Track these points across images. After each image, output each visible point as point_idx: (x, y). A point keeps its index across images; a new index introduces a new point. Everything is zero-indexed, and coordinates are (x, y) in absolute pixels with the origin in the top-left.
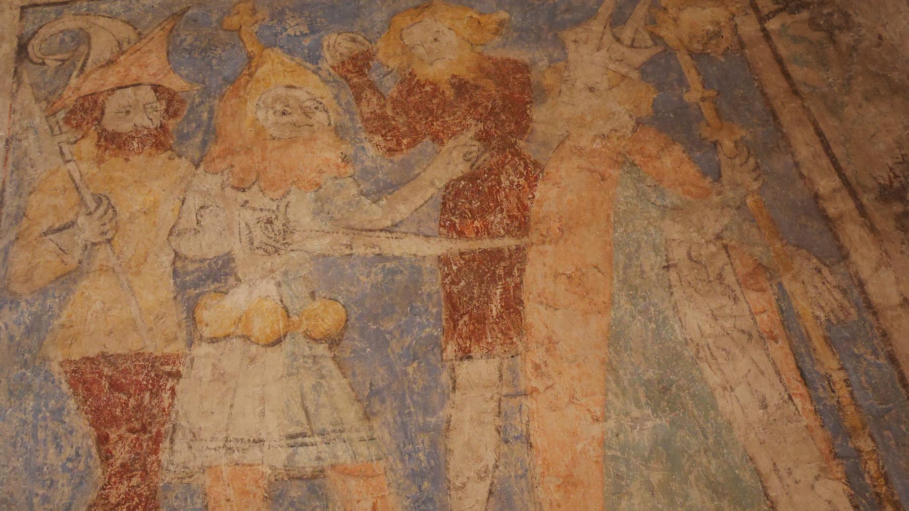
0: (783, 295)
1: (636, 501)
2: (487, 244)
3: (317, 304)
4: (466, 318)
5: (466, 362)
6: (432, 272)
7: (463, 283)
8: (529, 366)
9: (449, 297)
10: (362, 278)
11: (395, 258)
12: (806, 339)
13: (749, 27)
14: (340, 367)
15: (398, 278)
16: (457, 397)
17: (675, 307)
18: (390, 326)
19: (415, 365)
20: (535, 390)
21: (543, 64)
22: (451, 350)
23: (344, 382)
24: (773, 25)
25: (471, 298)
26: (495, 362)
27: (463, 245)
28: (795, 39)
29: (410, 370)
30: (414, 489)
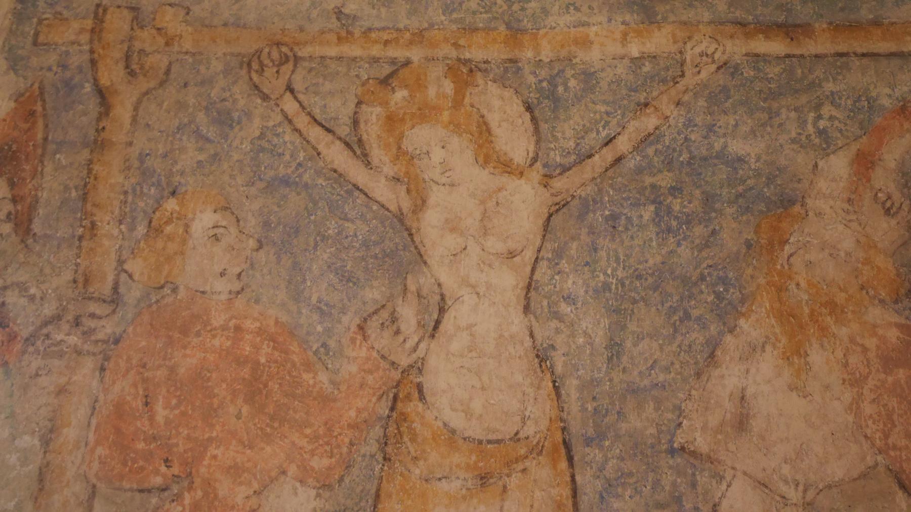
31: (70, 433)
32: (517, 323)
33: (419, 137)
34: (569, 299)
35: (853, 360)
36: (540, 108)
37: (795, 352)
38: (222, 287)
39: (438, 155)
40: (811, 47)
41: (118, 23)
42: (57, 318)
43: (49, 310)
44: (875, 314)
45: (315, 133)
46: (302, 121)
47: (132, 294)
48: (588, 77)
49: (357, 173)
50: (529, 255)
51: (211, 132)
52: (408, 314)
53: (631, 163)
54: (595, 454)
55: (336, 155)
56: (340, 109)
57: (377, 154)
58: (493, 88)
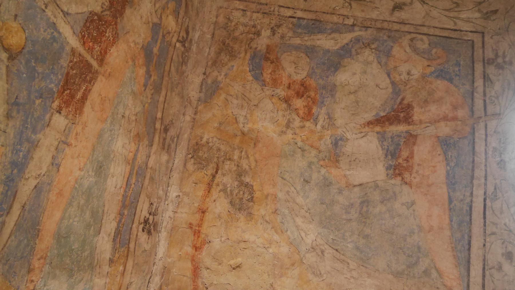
0: (137, 150)
1: (73, 210)
2: (88, 58)
3: (15, 25)
4: (68, 91)
5: (58, 114)
6: (67, 54)
7: (74, 72)
8: (75, 132)
9: (68, 73)
10: (42, 30)
11: (59, 33)
12: (134, 169)
14: (8, 76)
15: (55, 44)
16: (47, 130)
17: (118, 135)
18: (40, 70)
19: (40, 101)
20: (71, 145)
22: (56, 103)
23: (6, 86)
25: (74, 83)
26: (66, 121)
27: (81, 50)
29: (38, 102)
30: (10, 171)
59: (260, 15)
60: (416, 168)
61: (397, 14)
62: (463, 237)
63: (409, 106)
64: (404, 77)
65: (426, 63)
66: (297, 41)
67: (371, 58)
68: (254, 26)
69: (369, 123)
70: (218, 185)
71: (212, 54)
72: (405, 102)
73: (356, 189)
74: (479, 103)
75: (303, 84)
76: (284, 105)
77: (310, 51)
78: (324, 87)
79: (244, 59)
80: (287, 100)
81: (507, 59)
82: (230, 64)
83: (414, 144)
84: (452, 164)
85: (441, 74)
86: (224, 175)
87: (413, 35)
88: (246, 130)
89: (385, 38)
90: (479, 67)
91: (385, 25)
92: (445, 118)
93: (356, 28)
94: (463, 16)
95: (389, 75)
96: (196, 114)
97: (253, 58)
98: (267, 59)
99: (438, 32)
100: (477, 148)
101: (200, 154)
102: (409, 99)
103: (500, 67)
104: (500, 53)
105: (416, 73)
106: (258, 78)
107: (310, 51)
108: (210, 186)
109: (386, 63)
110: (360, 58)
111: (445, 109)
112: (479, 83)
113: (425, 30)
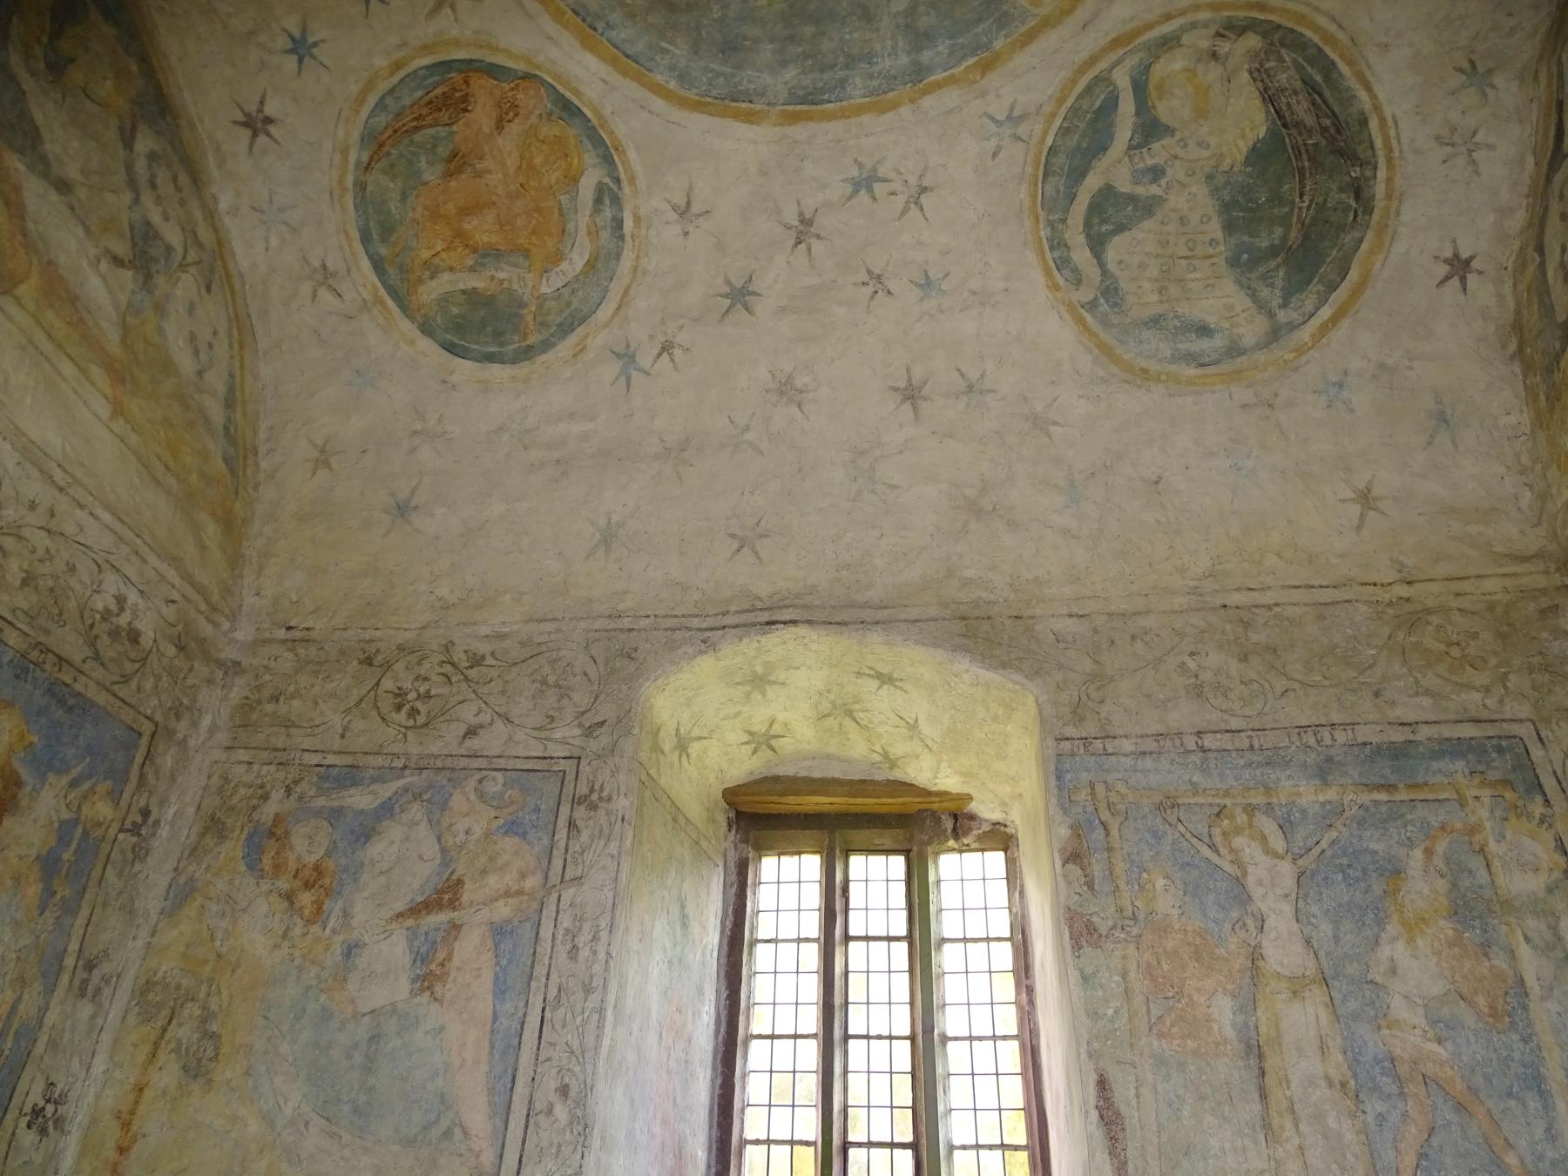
13: (112, 832)
21: (29, 788)
24: (121, 836)
28: (123, 852)
31: (1132, 975)
32: (1295, 927)
33: (1239, 842)
34: (1314, 916)
35: (1436, 944)
36: (1286, 827)
37: (1411, 940)
38: (1175, 912)
39: (1247, 851)
40: (1399, 797)
41: (1100, 789)
42: (1114, 927)
43: (1110, 923)
44: (1442, 923)
45: (1195, 841)
46: (1188, 835)
47: (1141, 916)
48: (1303, 812)
49: (1215, 859)
50: (1294, 896)
51: (1153, 842)
52: (1250, 921)
53: (1329, 853)
54: (1336, 983)
55: (1206, 852)
56: (1202, 829)
57: (1223, 851)
58: (1264, 817)
59: (272, 768)
60: (452, 975)
61: (468, 743)
62: (505, 1071)
63: (460, 882)
64: (461, 837)
65: (493, 813)
66: (321, 802)
67: (419, 816)
68: (262, 786)
69: (400, 915)
70: (169, 1042)
71: (193, 838)
72: (455, 877)
73: (366, 1019)
74: (557, 863)
75: (317, 868)
76: (286, 904)
77: (335, 816)
78: (346, 869)
79: (238, 839)
80: (289, 897)
81: (605, 794)
82: (217, 850)
83: (456, 938)
84: (504, 962)
85: (513, 828)
86: (180, 1025)
87: (484, 773)
88: (224, 950)
89: (444, 782)
90: (565, 810)
91: (449, 762)
92: (508, 894)
93: (407, 772)
94: (558, 735)
95: (439, 840)
96: (153, 935)
97: (251, 836)
98: (271, 834)
99: (520, 764)
100: (542, 933)
101: (150, 997)
102: (460, 871)
103: (593, 807)
104: (597, 787)
105: (478, 831)
106: (253, 865)
107: (335, 816)
108: (156, 1045)
109: (438, 821)
110: (405, 817)
111: (509, 880)
112: (562, 834)
113: (502, 763)
